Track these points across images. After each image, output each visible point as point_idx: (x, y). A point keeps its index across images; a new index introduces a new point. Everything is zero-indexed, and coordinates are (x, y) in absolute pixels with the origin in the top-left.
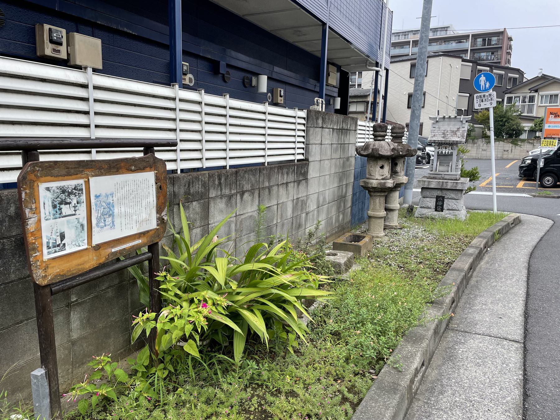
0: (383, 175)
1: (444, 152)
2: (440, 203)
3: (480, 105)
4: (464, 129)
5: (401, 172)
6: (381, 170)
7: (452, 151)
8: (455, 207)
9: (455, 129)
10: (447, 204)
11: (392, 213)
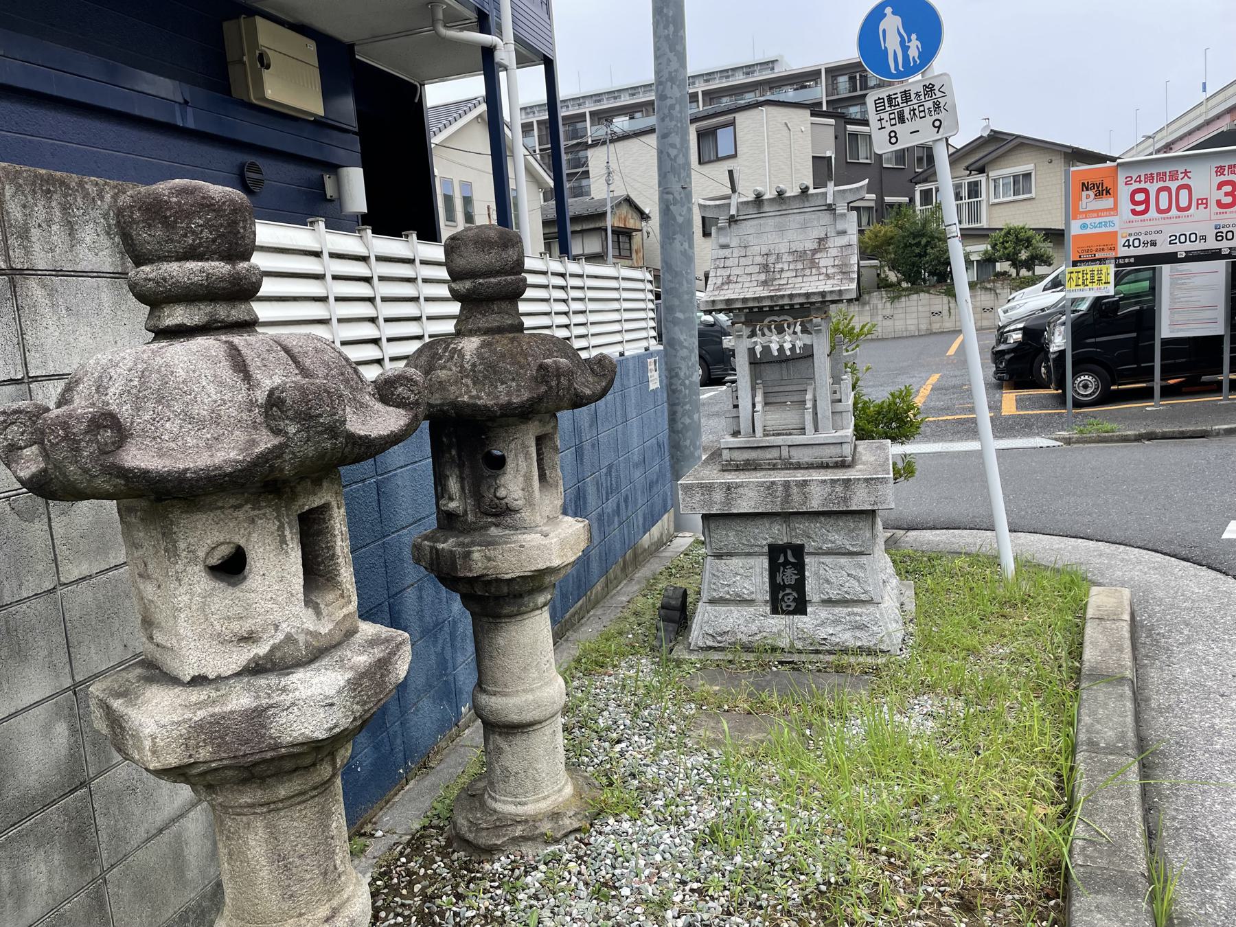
0: (249, 638)
1: (774, 347)
2: (789, 576)
3: (893, 137)
4: (843, 241)
5: (530, 503)
6: (223, 597)
7: (806, 339)
8: (853, 588)
9: (810, 245)
10: (820, 575)
11: (519, 741)
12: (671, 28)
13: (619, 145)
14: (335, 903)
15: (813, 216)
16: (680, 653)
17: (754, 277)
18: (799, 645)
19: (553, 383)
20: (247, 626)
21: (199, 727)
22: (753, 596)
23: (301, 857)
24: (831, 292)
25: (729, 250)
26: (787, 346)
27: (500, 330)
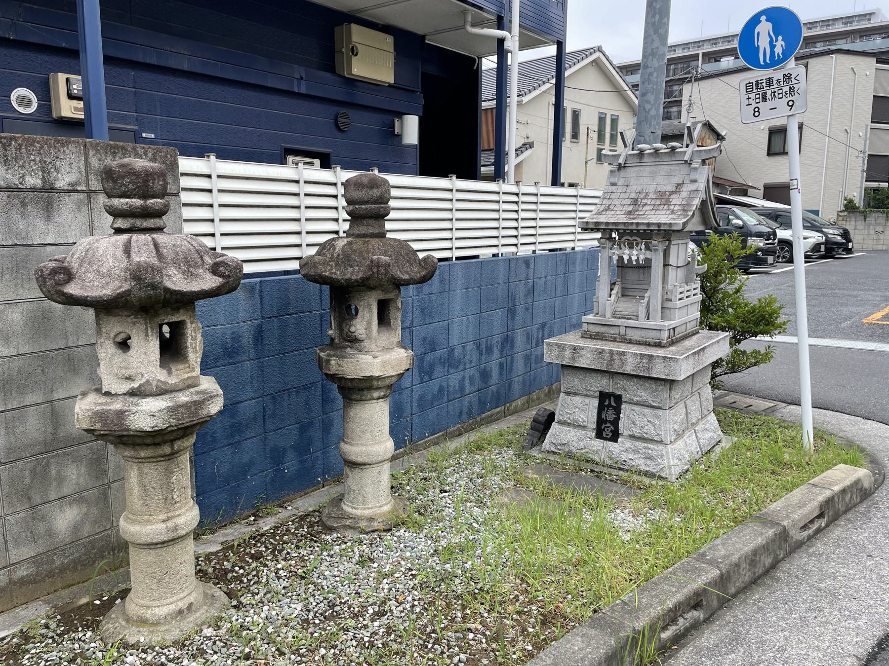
0: (129, 378)
1: (634, 258)
2: (610, 415)
4: (693, 187)
5: (369, 337)
6: (119, 357)
7: (649, 255)
8: (650, 431)
9: (671, 188)
10: (630, 418)
11: (356, 471)
12: (657, 17)
13: (703, 83)
14: (170, 515)
15: (677, 167)
16: (534, 452)
17: (625, 208)
18: (609, 462)
19: (375, 270)
20: (127, 373)
21: (96, 413)
22: (585, 424)
23: (153, 487)
24: (664, 224)
25: (616, 187)
26: (634, 258)
27: (373, 236)
